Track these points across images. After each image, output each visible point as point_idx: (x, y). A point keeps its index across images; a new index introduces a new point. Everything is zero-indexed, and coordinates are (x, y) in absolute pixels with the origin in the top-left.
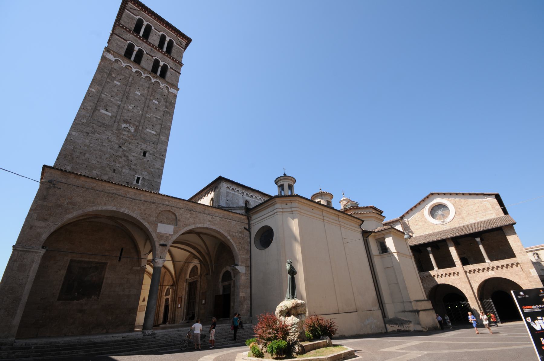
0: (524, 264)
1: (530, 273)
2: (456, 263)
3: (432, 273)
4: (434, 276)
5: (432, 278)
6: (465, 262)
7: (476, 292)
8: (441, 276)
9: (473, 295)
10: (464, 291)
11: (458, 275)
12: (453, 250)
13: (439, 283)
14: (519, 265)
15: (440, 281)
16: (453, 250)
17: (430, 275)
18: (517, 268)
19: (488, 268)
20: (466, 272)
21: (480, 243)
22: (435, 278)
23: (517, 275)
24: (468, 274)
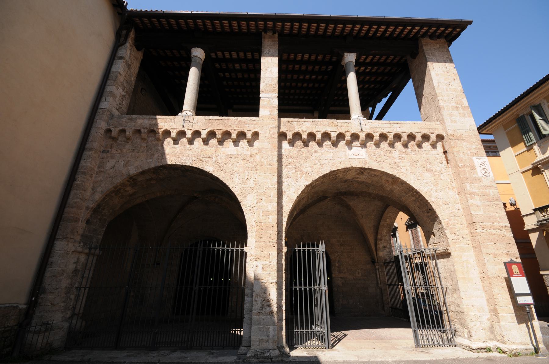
0: (459, 138)
1: (473, 167)
2: (263, 103)
3: (164, 122)
4: (167, 133)
5: (156, 137)
6: (288, 107)
7: (287, 207)
8: (189, 140)
9: (273, 219)
10: (247, 203)
11: (250, 143)
12: (270, 68)
13: (170, 160)
14: (439, 145)
15: (176, 154)
16: (270, 68)
17: (153, 131)
18: (434, 151)
19: (355, 137)
20: (282, 136)
21: (352, 66)
22: (168, 142)
23: (429, 171)
24: (285, 144)
